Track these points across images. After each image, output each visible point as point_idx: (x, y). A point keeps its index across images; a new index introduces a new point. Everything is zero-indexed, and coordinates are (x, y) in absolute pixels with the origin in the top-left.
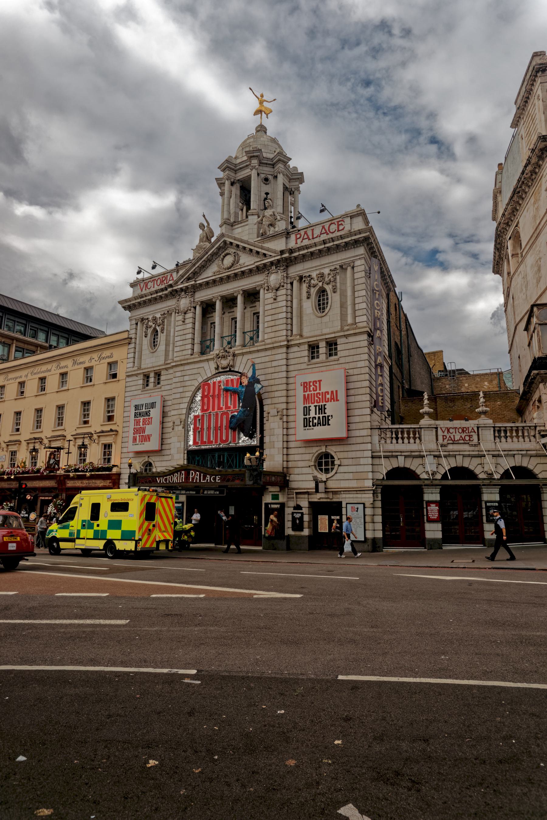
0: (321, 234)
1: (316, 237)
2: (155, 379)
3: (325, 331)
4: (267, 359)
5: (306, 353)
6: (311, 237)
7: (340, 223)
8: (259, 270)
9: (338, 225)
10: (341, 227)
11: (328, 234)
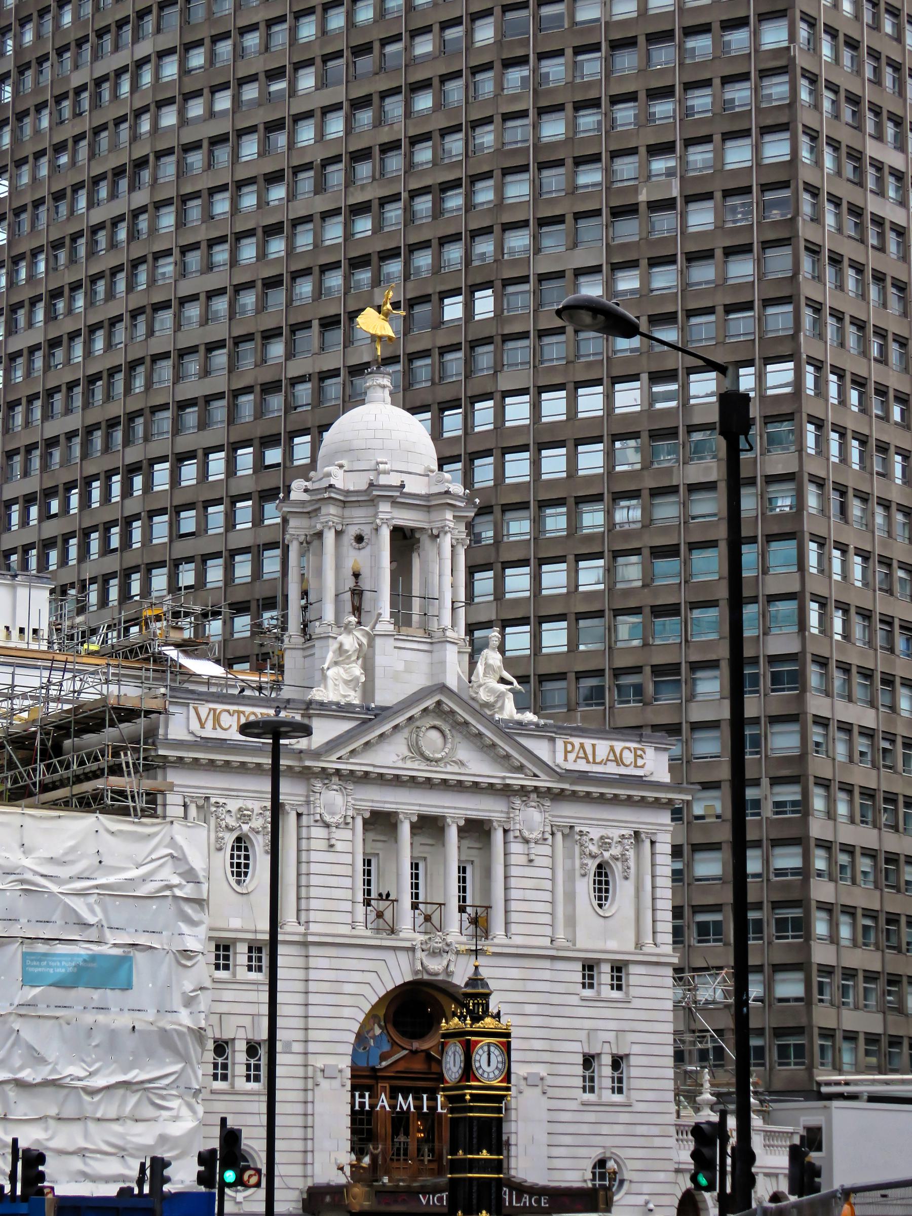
0: (608, 760)
1: (600, 763)
2: (250, 959)
3: (612, 945)
4: (515, 973)
5: (578, 977)
6: (591, 760)
7: (639, 752)
8: (506, 791)
9: (636, 756)
10: (640, 762)
11: (618, 765)
